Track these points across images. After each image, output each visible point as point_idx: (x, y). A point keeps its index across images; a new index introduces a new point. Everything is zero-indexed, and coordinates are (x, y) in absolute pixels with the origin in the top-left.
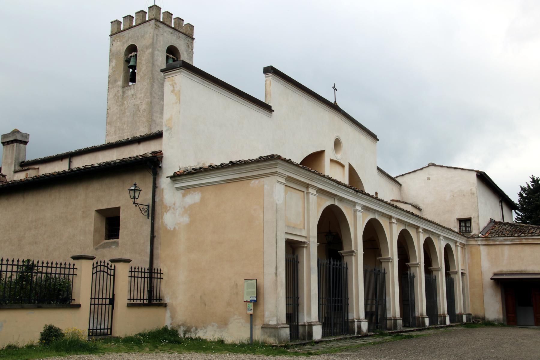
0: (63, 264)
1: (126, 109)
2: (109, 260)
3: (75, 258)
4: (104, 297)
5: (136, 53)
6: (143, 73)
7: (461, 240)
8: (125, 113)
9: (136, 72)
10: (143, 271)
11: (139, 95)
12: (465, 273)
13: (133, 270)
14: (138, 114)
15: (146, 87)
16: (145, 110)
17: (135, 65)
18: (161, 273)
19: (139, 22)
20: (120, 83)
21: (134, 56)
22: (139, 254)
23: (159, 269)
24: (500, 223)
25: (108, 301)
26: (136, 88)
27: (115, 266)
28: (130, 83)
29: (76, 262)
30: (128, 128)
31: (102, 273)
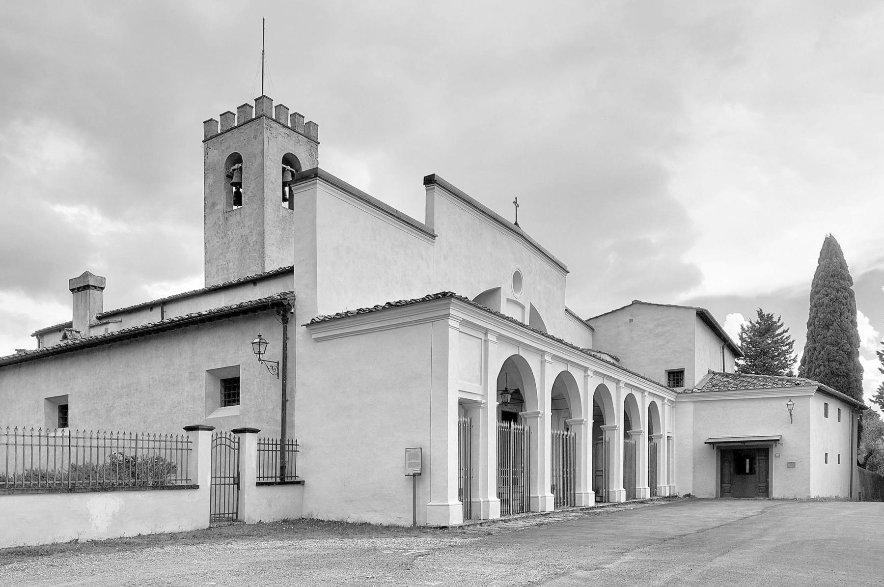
0: (174, 436)
1: (230, 242)
2: (232, 431)
3: (189, 429)
4: (223, 475)
5: (240, 165)
6: (251, 192)
7: (669, 395)
8: (229, 247)
9: (241, 192)
10: (274, 443)
11: (247, 223)
12: (671, 437)
13: (262, 442)
14: (247, 248)
15: (256, 211)
16: (256, 242)
17: (240, 181)
18: (296, 445)
19: (242, 121)
20: (221, 205)
21: (237, 169)
22: (267, 423)
23: (294, 441)
24: (719, 374)
25: (232, 480)
26: (242, 214)
27: (239, 438)
28: (234, 206)
29: (191, 433)
30: (235, 267)
31: (223, 446)
